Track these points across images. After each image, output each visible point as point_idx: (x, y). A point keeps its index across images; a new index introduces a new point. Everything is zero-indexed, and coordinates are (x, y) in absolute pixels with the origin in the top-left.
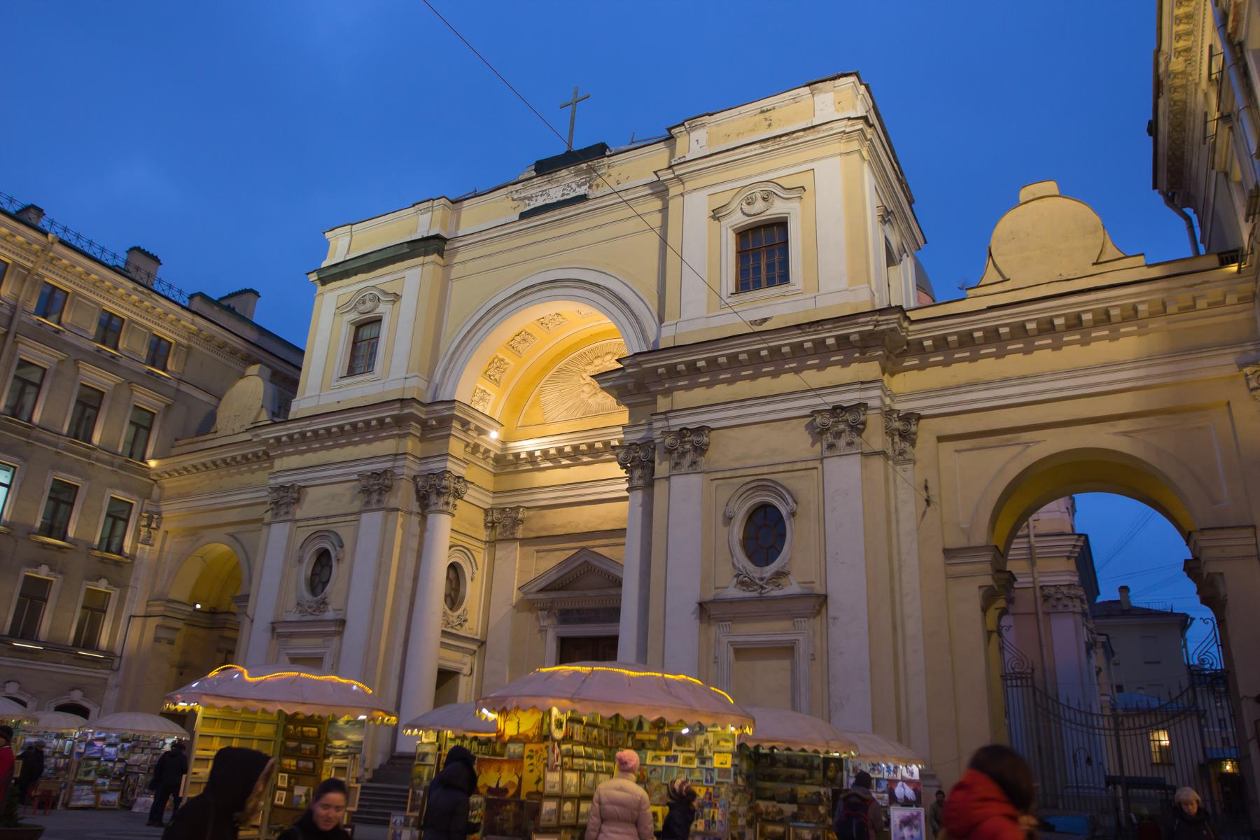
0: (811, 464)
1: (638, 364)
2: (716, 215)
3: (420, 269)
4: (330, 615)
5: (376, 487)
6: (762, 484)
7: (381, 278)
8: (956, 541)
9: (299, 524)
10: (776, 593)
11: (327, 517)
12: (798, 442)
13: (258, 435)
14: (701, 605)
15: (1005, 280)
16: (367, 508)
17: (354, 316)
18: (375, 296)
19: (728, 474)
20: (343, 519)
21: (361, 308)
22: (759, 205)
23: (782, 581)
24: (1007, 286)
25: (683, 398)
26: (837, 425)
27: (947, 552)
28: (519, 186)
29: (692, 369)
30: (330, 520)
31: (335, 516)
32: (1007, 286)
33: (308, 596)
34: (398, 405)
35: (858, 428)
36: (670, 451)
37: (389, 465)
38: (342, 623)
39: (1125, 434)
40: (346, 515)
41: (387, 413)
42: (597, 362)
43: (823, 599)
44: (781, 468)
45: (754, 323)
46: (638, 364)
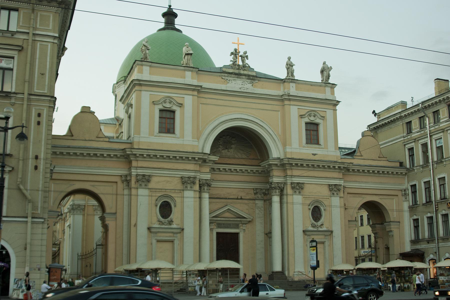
0: (328, 197)
1: (289, 161)
2: (301, 116)
3: (191, 96)
4: (174, 226)
5: (187, 182)
6: (317, 201)
7: (175, 95)
8: (350, 220)
9: (152, 190)
10: (320, 229)
11: (166, 189)
12: (325, 191)
13: (131, 151)
14: (303, 231)
15: (361, 156)
16: (186, 189)
17: (161, 107)
18: (171, 101)
19: (308, 197)
20: (174, 191)
21: (165, 105)
22: (312, 118)
23: (322, 226)
24: (362, 158)
25: (296, 172)
26: (334, 189)
27: (349, 221)
28: (226, 75)
29: (302, 165)
30: (167, 191)
31: (170, 190)
32: (362, 158)
33: (162, 219)
34: (203, 155)
35: (339, 190)
36: (293, 188)
37: (194, 174)
38: (183, 229)
39: (381, 199)
40: (175, 190)
41: (197, 157)
42: (224, 137)
43: (332, 232)
44: (321, 197)
45: (313, 154)
46: (289, 161)
